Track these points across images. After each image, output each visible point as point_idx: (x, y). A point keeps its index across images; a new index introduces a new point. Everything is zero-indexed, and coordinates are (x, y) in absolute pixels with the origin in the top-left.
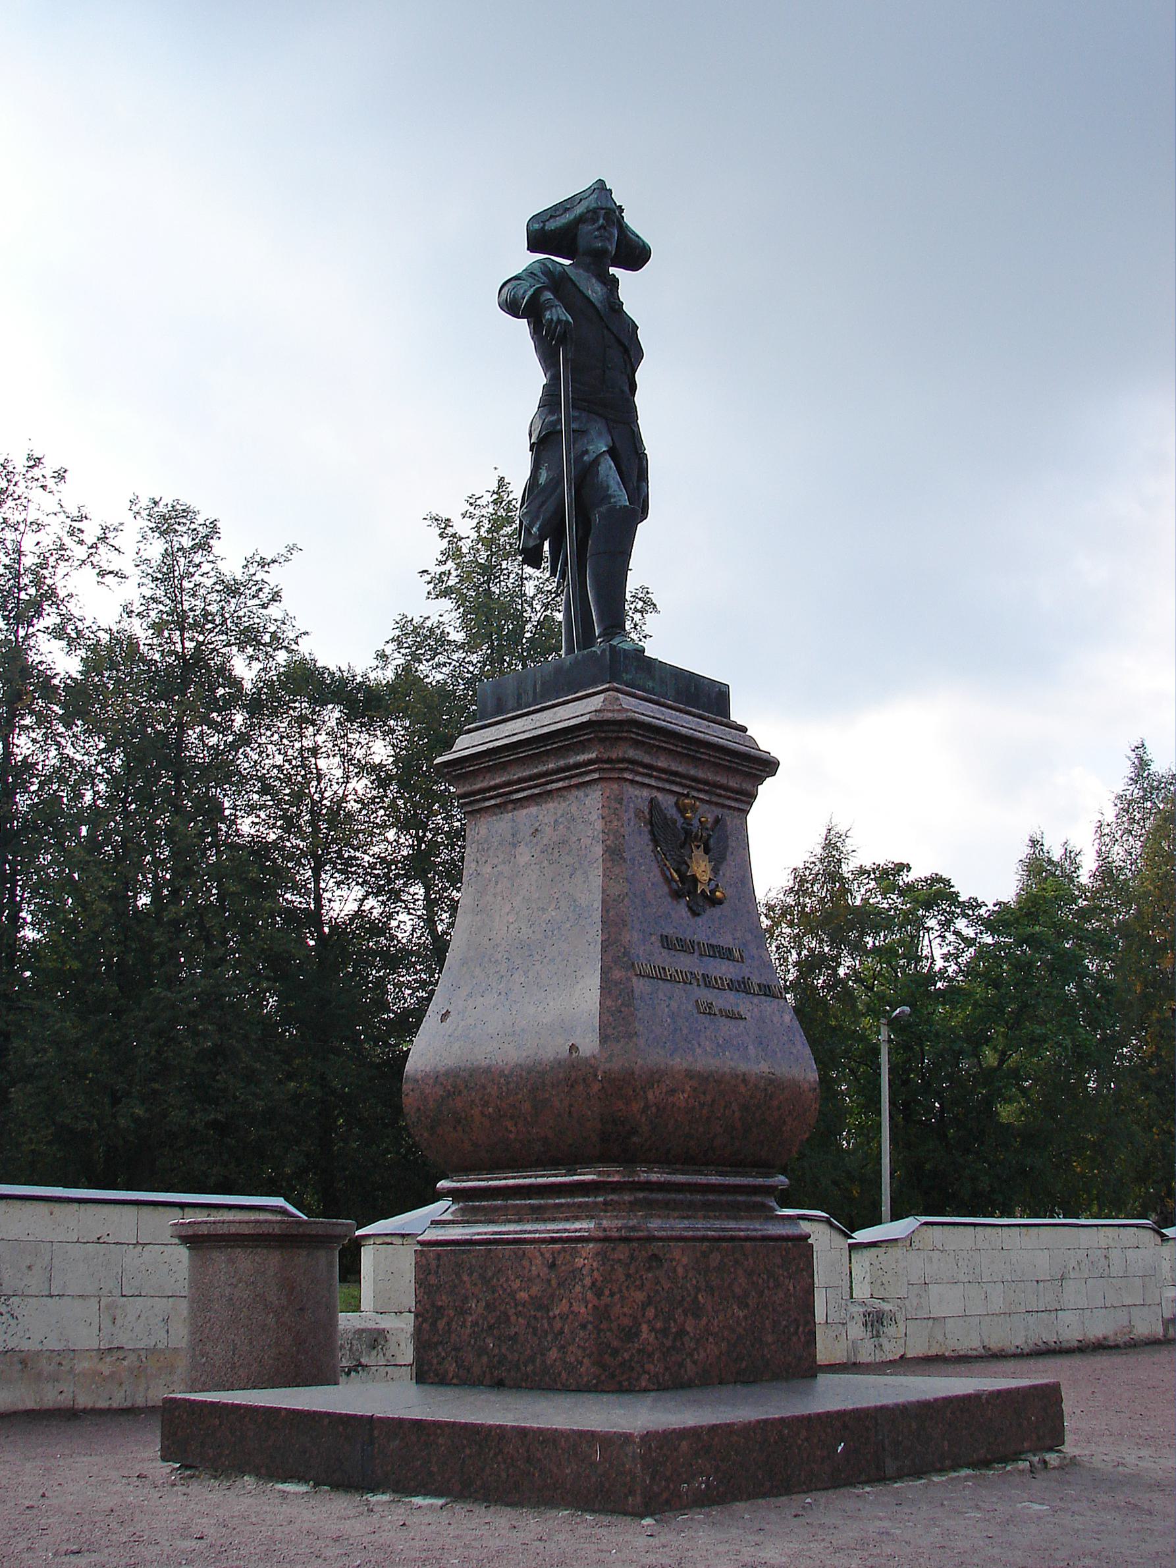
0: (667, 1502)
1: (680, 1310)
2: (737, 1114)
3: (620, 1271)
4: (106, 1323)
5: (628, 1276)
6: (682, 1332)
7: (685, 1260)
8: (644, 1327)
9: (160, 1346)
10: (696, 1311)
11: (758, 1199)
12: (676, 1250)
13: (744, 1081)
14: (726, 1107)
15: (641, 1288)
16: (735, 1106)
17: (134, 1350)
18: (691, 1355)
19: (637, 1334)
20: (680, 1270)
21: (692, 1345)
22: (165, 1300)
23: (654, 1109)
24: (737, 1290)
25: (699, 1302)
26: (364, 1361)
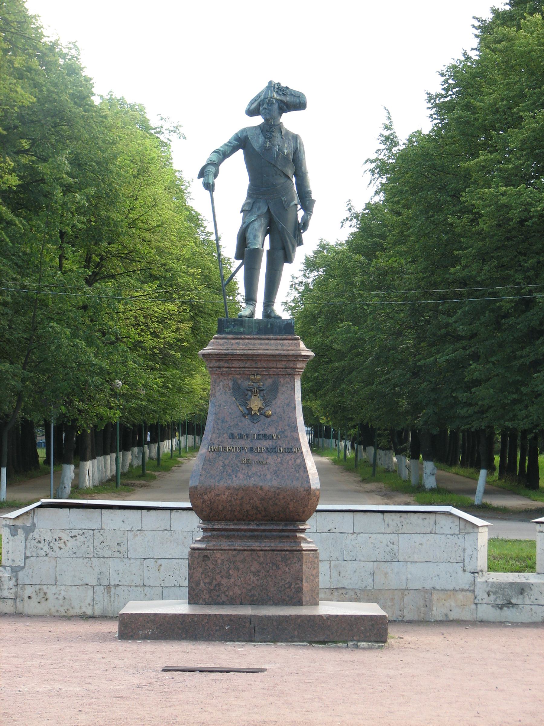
0: (132, 636)
1: (219, 576)
2: (258, 502)
3: (196, 561)
4: (335, 573)
5: (198, 563)
6: (219, 584)
7: (223, 558)
8: (202, 581)
9: (369, 587)
10: (229, 577)
11: (292, 534)
12: (218, 554)
13: (261, 489)
14: (250, 500)
15: (201, 567)
16: (255, 499)
17: (352, 589)
18: (224, 593)
19: (200, 584)
20: (219, 562)
21: (226, 589)
22: (372, 563)
23: (209, 502)
24: (253, 570)
25: (230, 574)
26: (514, 601)
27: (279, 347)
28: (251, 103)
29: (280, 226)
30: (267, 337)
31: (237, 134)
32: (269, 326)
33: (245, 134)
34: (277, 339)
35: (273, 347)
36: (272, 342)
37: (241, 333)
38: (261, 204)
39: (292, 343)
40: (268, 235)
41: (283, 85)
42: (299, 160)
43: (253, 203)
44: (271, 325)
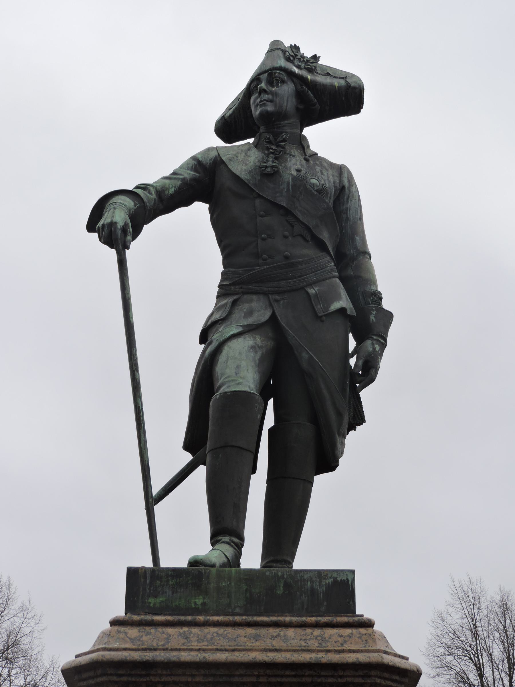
27: (314, 644)
28: (229, 109)
29: (305, 355)
30: (274, 619)
31: (194, 158)
32: (280, 591)
33: (214, 154)
34: (303, 625)
35: (295, 643)
36: (291, 632)
37: (197, 611)
38: (254, 305)
39: (350, 636)
40: (272, 399)
41: (307, 52)
42: (348, 219)
43: (234, 303)
44: (287, 585)
